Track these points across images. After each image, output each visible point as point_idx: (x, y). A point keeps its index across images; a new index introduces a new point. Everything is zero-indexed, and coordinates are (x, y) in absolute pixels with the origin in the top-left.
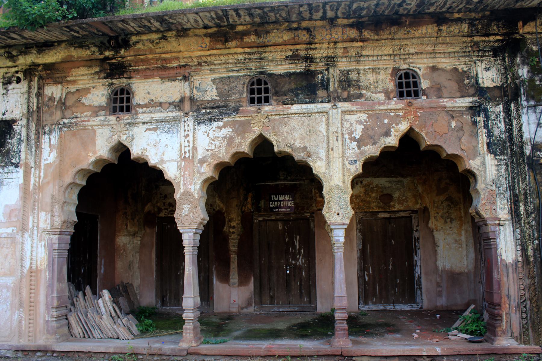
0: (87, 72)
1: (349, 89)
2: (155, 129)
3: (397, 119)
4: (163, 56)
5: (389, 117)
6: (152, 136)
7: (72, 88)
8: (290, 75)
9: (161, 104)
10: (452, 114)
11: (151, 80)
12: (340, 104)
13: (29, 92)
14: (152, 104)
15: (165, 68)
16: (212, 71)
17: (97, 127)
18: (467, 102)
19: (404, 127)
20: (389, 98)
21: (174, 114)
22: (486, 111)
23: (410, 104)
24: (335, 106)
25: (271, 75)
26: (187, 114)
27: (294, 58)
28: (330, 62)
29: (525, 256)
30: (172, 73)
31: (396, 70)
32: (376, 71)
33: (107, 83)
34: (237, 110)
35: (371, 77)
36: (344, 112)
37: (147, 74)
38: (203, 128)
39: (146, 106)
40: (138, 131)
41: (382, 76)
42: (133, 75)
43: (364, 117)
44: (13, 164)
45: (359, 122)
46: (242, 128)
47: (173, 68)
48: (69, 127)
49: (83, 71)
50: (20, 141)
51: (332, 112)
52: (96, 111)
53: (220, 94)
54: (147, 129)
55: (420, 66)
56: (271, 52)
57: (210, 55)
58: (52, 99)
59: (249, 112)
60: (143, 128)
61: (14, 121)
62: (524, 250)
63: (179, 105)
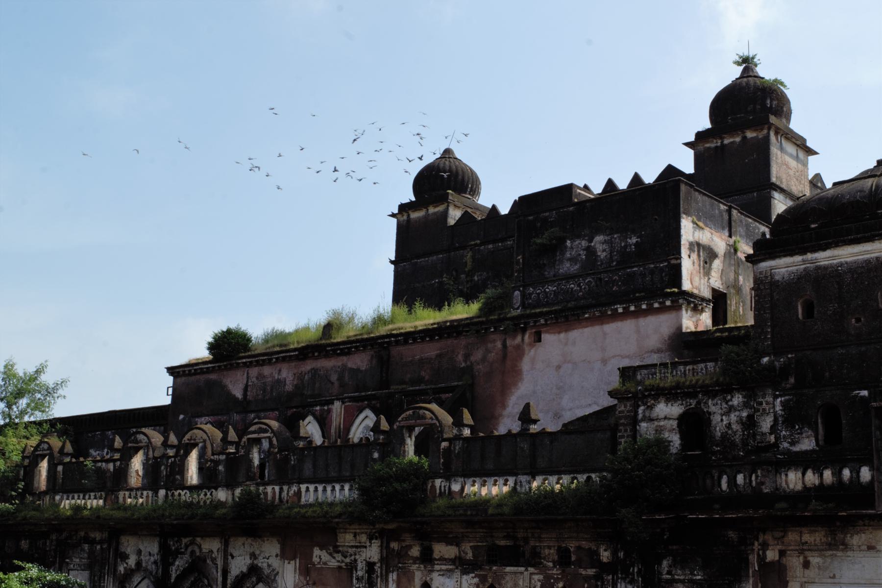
1: (533, 560)
2: (443, 575)
3: (557, 580)
5: (553, 578)
6: (442, 579)
7: (404, 544)
8: (506, 546)
9: (445, 559)
10: (587, 578)
12: (529, 569)
13: (381, 546)
14: (443, 560)
16: (470, 542)
18: (591, 572)
19: (561, 585)
20: (555, 566)
21: (451, 567)
22: (603, 578)
23: (563, 571)
24: (527, 570)
25: (499, 546)
26: (457, 568)
27: (507, 537)
28: (526, 540)
31: (559, 547)
32: (549, 547)
34: (481, 568)
35: (547, 551)
36: (531, 574)
37: (439, 541)
38: (465, 577)
39: (439, 560)
40: (435, 575)
41: (552, 551)
43: (541, 577)
45: (539, 580)
46: (483, 579)
50: (377, 577)
51: (526, 573)
52: (415, 560)
53: (474, 556)
55: (572, 545)
58: (393, 550)
60: (437, 574)
61: (374, 564)
63: (453, 561)
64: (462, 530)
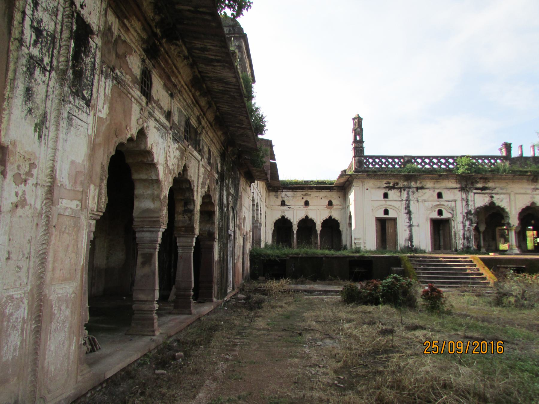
0: (139, 31)
2: (158, 129)
4: (174, 67)
11: (160, 80)
15: (169, 79)
17: (133, 100)
29: (220, 257)
30: (170, 85)
33: (142, 57)
42: (156, 65)
44: (84, 98)
47: (172, 82)
48: (119, 83)
49: (138, 26)
54: (155, 127)
56: (197, 108)
57: (185, 89)
59: (186, 144)
62: (220, 254)
64: (183, 83)
